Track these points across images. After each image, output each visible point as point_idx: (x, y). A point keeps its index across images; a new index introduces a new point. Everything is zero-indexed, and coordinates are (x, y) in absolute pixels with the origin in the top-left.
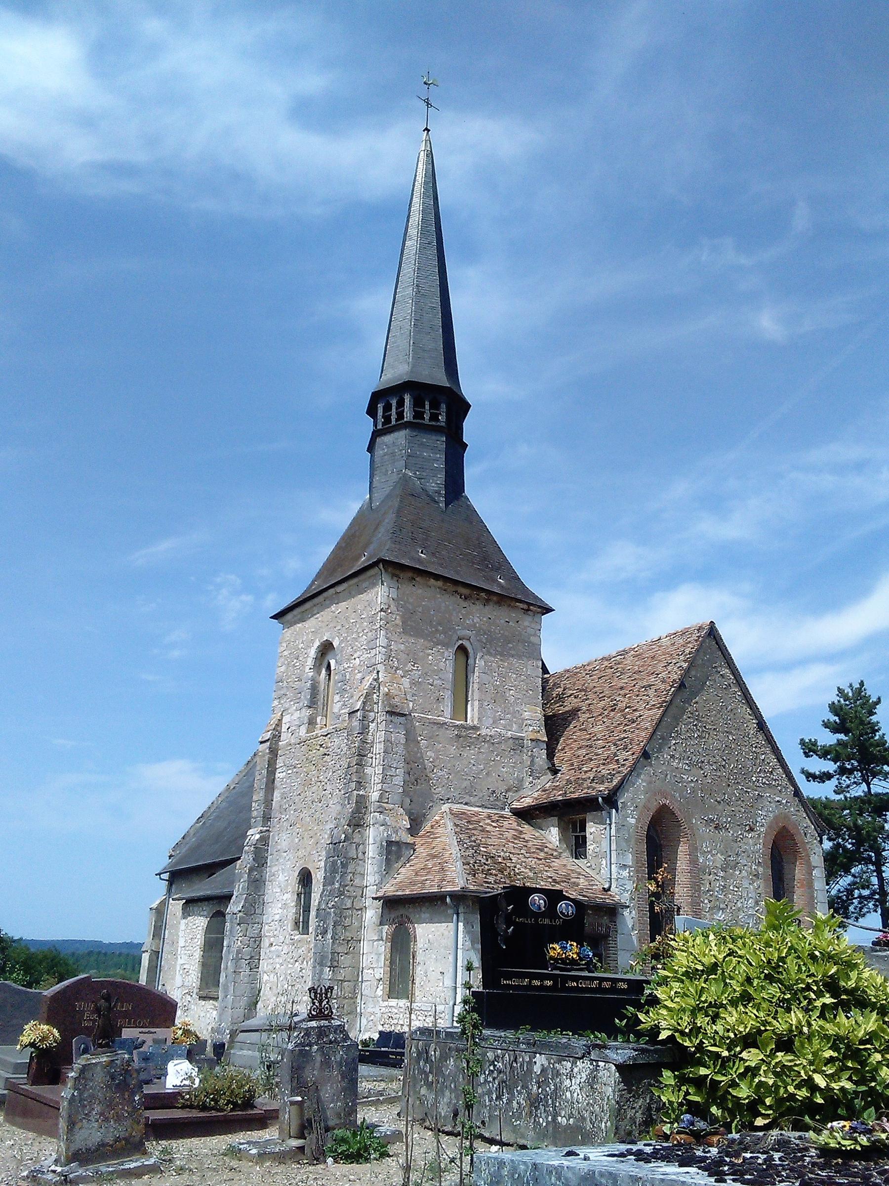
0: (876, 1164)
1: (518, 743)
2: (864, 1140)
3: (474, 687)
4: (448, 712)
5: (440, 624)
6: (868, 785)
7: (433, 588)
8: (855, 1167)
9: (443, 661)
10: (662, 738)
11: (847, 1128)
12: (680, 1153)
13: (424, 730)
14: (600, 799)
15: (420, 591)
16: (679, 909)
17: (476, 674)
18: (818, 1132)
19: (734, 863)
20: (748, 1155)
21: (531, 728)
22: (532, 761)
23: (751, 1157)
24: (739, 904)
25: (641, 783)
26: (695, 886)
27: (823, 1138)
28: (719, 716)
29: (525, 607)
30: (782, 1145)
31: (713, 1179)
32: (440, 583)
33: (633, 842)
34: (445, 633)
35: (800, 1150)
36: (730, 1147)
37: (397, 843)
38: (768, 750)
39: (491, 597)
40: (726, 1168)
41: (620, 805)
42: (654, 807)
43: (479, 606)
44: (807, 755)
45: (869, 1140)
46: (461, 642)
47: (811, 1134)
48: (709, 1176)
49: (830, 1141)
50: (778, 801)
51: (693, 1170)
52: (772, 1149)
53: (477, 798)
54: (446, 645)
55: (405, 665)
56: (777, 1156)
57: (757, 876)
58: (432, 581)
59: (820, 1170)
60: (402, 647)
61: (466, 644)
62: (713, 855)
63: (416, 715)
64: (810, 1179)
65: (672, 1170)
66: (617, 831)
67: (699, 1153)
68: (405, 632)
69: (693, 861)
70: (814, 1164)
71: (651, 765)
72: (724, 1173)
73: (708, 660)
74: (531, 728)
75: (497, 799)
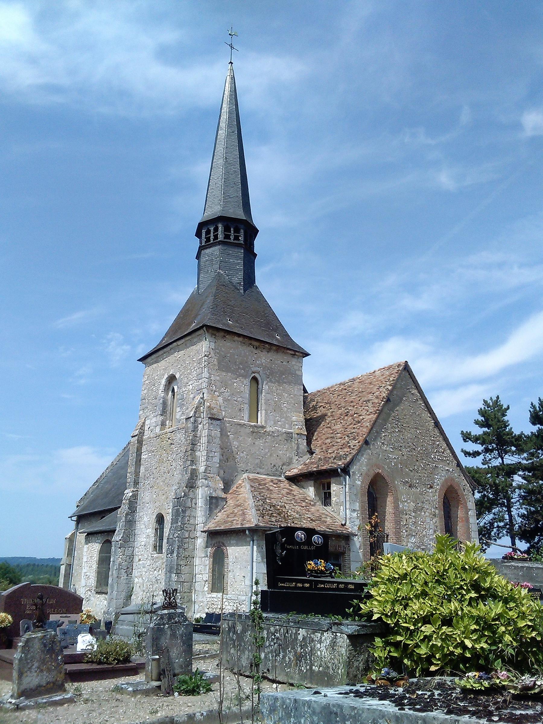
0: (493, 698)
1: (289, 436)
2: (486, 684)
3: (262, 401)
4: (246, 417)
5: (241, 364)
6: (502, 459)
7: (236, 342)
8: (481, 700)
9: (243, 386)
10: (377, 432)
11: (477, 677)
12: (380, 692)
13: (232, 428)
14: (339, 470)
16: (388, 536)
17: (263, 394)
18: (461, 678)
20: (420, 693)
21: (297, 427)
22: (298, 448)
23: (422, 694)
24: (424, 533)
26: (397, 522)
27: (463, 683)
28: (411, 418)
29: (293, 353)
30: (441, 686)
31: (397, 708)
32: (241, 339)
33: (359, 496)
35: (450, 689)
36: (410, 688)
37: (216, 498)
38: (441, 439)
40: (406, 701)
42: (372, 474)
44: (465, 441)
45: (489, 683)
46: (254, 375)
47: (457, 679)
48: (396, 706)
49: (467, 684)
51: (386, 702)
52: (434, 689)
53: (264, 470)
54: (245, 377)
55: (220, 389)
56: (436, 692)
57: (435, 515)
58: (236, 338)
59: (460, 702)
61: (257, 375)
63: (227, 419)
64: (453, 708)
65: (374, 703)
66: (350, 489)
67: (391, 692)
68: (219, 369)
69: (396, 507)
70: (457, 698)
72: (404, 705)
73: (404, 384)
74: (297, 427)
75: (277, 470)
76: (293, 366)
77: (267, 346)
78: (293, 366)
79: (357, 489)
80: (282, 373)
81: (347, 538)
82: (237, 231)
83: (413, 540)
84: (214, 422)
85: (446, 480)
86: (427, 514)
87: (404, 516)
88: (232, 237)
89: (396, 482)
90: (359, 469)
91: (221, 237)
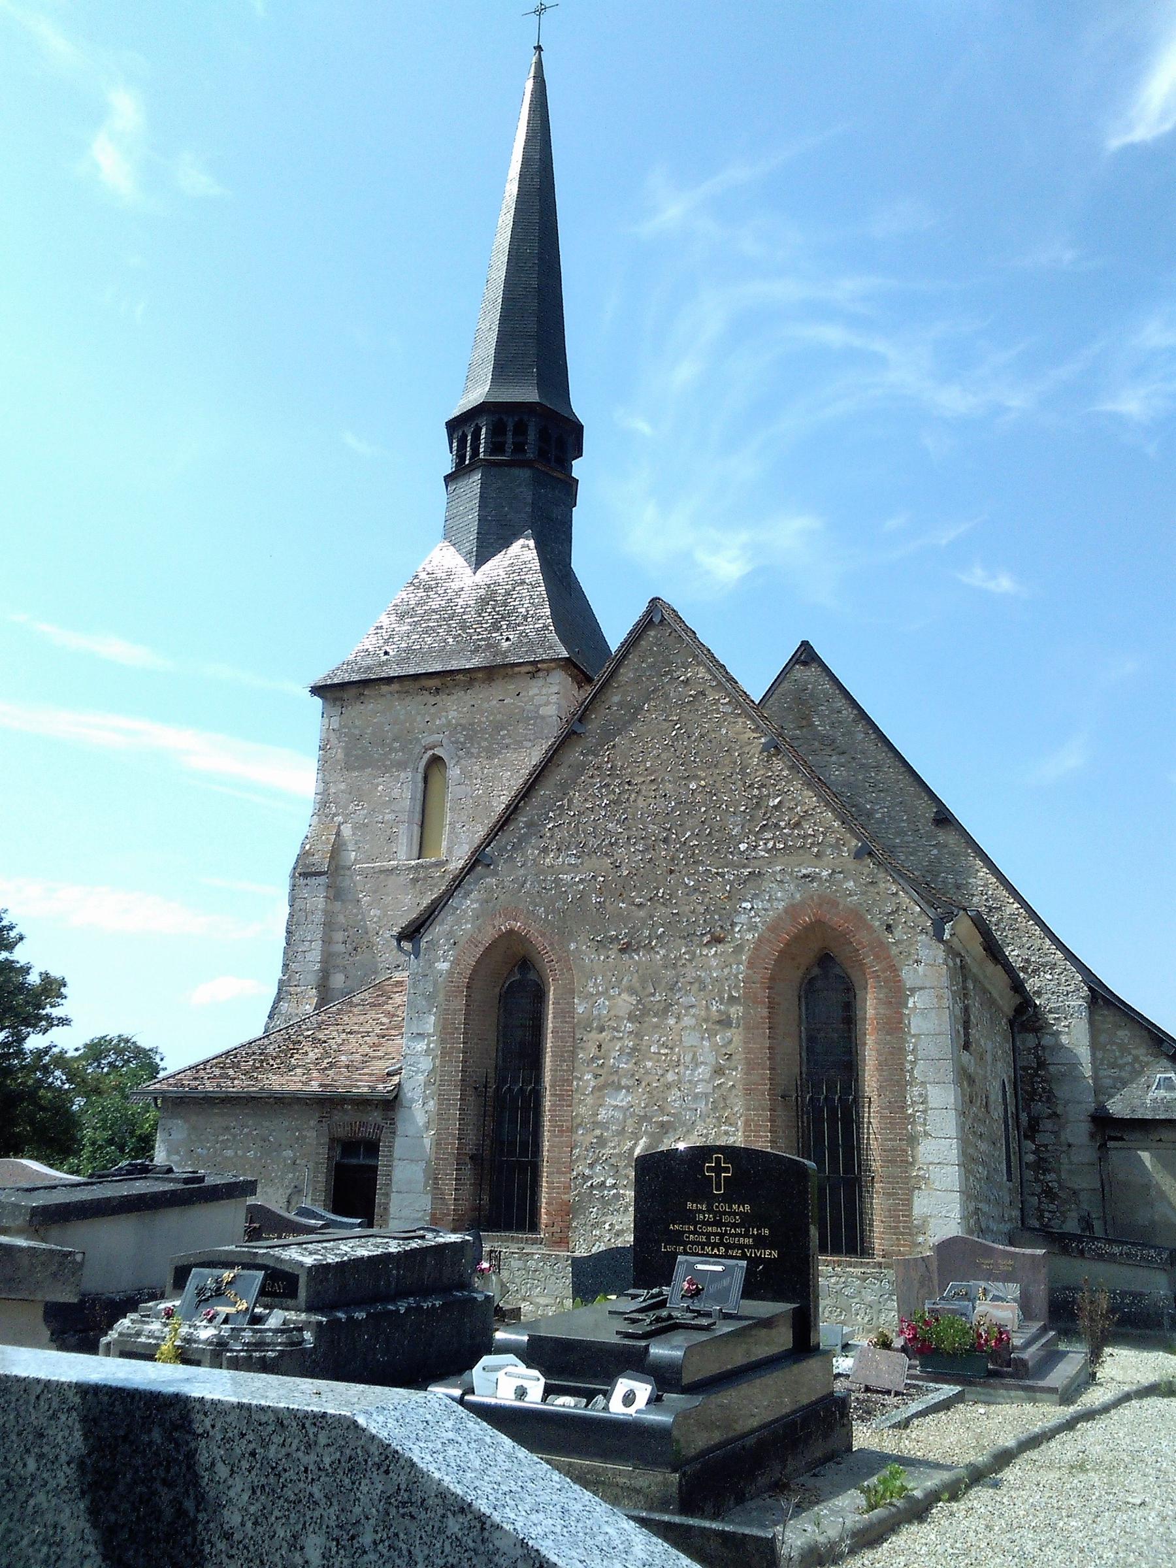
9: (401, 789)
10: (530, 825)
13: (367, 883)
19: (663, 1005)
24: (670, 1077)
25: (468, 904)
29: (529, 668)
32: (395, 687)
33: (441, 997)
41: (423, 945)
46: (430, 753)
50: (805, 876)
54: (401, 765)
55: (346, 808)
57: (725, 1022)
58: (385, 689)
60: (343, 786)
61: (438, 751)
62: (610, 998)
68: (348, 767)
71: (495, 873)
73: (652, 666)
76: (532, 699)
77: (460, 677)
78: (532, 699)
79: (435, 984)
80: (498, 727)
81: (391, 1104)
82: (520, 429)
83: (622, 1099)
84: (312, 881)
85: (792, 911)
86: (688, 1021)
87: (594, 1035)
88: (509, 447)
89: (573, 946)
90: (451, 932)
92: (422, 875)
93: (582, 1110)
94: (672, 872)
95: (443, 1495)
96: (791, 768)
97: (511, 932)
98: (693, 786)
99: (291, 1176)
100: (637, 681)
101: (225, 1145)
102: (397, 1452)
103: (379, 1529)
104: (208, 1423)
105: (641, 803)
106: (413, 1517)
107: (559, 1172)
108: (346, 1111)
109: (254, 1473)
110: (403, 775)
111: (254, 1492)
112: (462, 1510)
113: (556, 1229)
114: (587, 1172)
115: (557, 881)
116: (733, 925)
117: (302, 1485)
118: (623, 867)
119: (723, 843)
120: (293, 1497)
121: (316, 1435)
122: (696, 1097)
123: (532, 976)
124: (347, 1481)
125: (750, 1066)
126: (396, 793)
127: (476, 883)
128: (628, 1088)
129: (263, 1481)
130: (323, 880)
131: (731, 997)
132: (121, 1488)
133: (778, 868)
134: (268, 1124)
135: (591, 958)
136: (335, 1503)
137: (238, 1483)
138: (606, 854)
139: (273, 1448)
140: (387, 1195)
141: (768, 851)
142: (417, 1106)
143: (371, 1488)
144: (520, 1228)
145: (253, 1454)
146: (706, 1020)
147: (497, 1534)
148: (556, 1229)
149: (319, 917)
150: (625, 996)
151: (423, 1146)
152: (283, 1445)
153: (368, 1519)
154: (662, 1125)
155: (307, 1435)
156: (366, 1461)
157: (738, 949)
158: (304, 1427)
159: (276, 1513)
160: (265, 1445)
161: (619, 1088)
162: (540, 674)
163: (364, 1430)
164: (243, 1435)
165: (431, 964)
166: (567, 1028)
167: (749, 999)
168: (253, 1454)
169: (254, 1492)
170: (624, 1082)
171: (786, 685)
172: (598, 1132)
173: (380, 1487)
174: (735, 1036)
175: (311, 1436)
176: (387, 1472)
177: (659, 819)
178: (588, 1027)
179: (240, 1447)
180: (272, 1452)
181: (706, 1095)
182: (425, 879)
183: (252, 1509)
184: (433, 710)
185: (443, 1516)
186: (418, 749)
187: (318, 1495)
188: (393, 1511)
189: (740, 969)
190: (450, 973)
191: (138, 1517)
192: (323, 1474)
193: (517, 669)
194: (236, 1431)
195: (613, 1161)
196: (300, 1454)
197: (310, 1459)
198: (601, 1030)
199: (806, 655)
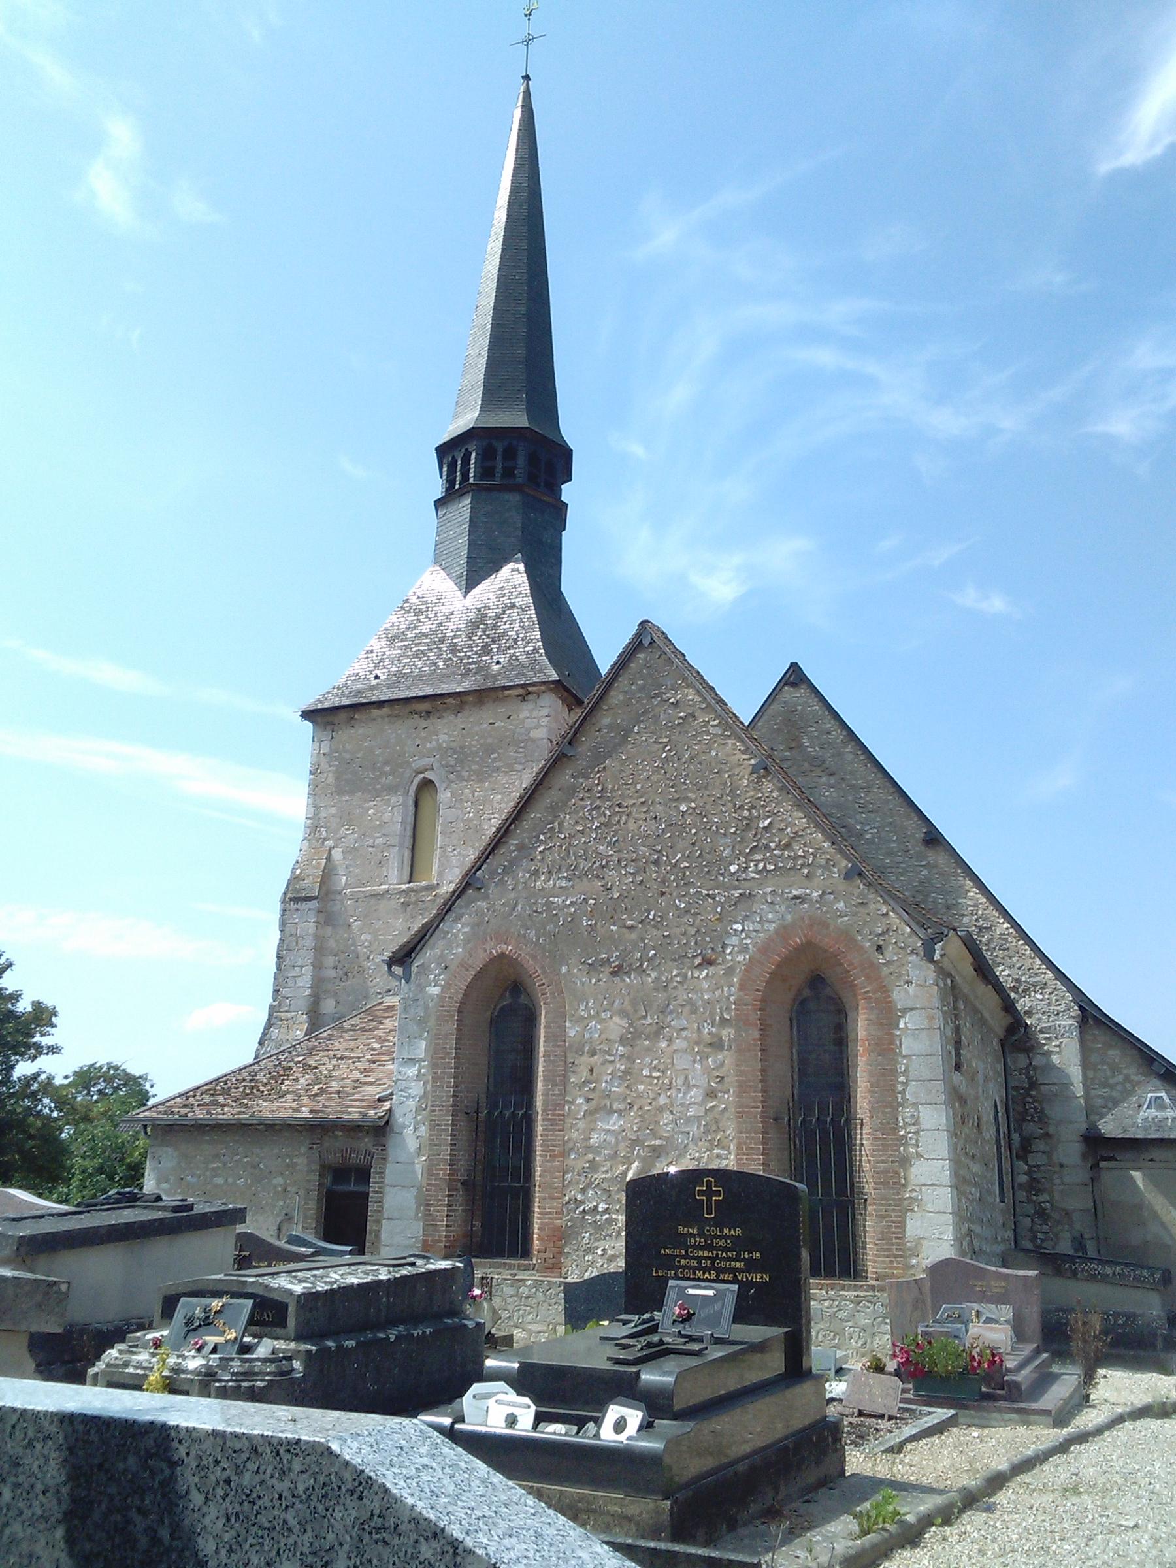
5: (387, 763)
9: (392, 813)
10: (521, 847)
15: (361, 731)
19: (655, 1027)
24: (663, 1100)
25: (458, 928)
32: (386, 710)
33: (432, 1022)
34: (393, 772)
39: (464, 699)
41: (414, 969)
43: (450, 718)
46: (421, 776)
50: (796, 897)
54: (392, 789)
55: (336, 831)
57: (716, 1045)
58: (375, 712)
60: (333, 810)
61: (429, 775)
68: (340, 791)
71: (486, 897)
73: (642, 689)
77: (450, 700)
78: (522, 722)
79: (426, 1008)
80: (489, 750)
81: (382, 1130)
82: (510, 454)
83: (614, 1123)
84: (304, 906)
85: (784, 932)
86: (679, 1044)
87: (585, 1059)
89: (564, 969)
90: (442, 956)
91: (520, 477)
92: (413, 899)
93: (575, 1135)
94: (663, 894)
95: (417, 1520)
96: (780, 789)
97: (502, 955)
98: (683, 808)
99: (281, 1203)
100: (627, 703)
101: (215, 1173)
102: (370, 1478)
103: (353, 1556)
104: (182, 1451)
105: (631, 825)
106: (386, 1543)
107: (553, 1198)
108: (336, 1137)
109: (228, 1500)
110: (394, 799)
111: (228, 1520)
112: (435, 1535)
113: (548, 1255)
114: (579, 1197)
115: (549, 904)
116: (724, 946)
117: (276, 1512)
118: (614, 890)
119: (712, 866)
120: (266, 1525)
121: (290, 1462)
122: (688, 1120)
123: (523, 1000)
124: (320, 1508)
125: (742, 1088)
126: (387, 817)
127: (467, 906)
128: (620, 1112)
129: (238, 1508)
130: (314, 904)
131: (723, 1021)
132: (96, 1516)
133: (769, 889)
134: (258, 1151)
135: (583, 981)
136: (309, 1529)
137: (213, 1510)
138: (598, 877)
139: (247, 1476)
140: (378, 1222)
141: (759, 872)
142: (408, 1132)
143: (345, 1514)
144: (513, 1254)
145: (228, 1481)
146: (697, 1043)
147: (470, 1559)
148: (548, 1255)
149: (309, 942)
150: (616, 1019)
151: (414, 1172)
152: (258, 1472)
153: (341, 1545)
154: (654, 1149)
155: (281, 1462)
156: (340, 1487)
157: (730, 971)
158: (278, 1453)
159: (251, 1540)
160: (239, 1471)
161: (611, 1111)
162: (530, 697)
163: (337, 1456)
164: (217, 1462)
165: (421, 988)
166: (559, 1051)
167: (740, 1021)
168: (228, 1481)
169: (228, 1520)
170: (616, 1106)
171: (776, 707)
172: (590, 1156)
173: (354, 1514)
174: (726, 1057)
175: (285, 1462)
176: (360, 1498)
177: (650, 841)
178: (580, 1051)
179: (216, 1474)
180: (247, 1479)
181: (699, 1118)
182: (415, 903)
183: (227, 1537)
184: (423, 734)
185: (417, 1542)
186: (408, 773)
187: (293, 1522)
188: (366, 1538)
189: (732, 991)
190: (441, 997)
191: (113, 1546)
192: (297, 1501)
193: (507, 692)
194: (211, 1459)
195: (605, 1185)
196: (274, 1481)
197: (283, 1486)
198: (593, 1053)
199: (795, 677)
